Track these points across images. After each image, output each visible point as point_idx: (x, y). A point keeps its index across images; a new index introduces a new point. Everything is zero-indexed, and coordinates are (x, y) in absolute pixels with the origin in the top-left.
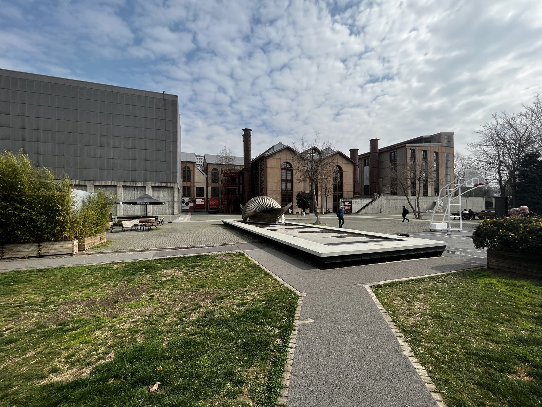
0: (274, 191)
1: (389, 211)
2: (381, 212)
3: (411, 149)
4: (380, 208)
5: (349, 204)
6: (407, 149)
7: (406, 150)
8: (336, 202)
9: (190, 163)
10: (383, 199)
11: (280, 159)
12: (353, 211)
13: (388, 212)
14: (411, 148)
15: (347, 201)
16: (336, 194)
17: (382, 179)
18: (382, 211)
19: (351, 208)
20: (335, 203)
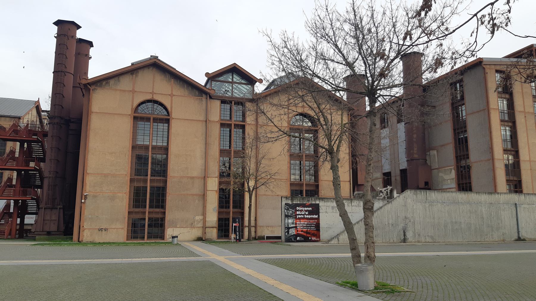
0: (106, 175)
1: (432, 237)
2: (405, 240)
3: (497, 71)
4: (401, 226)
5: (310, 213)
6: (487, 71)
7: (485, 73)
8: (229, 208)
9: (8, 119)
10: (409, 201)
11: (133, 92)
12: (324, 234)
13: (428, 239)
14: (498, 68)
15: (304, 206)
16: (138, 181)
17: (435, 152)
18: (409, 235)
19: (318, 226)
20: (224, 210)
